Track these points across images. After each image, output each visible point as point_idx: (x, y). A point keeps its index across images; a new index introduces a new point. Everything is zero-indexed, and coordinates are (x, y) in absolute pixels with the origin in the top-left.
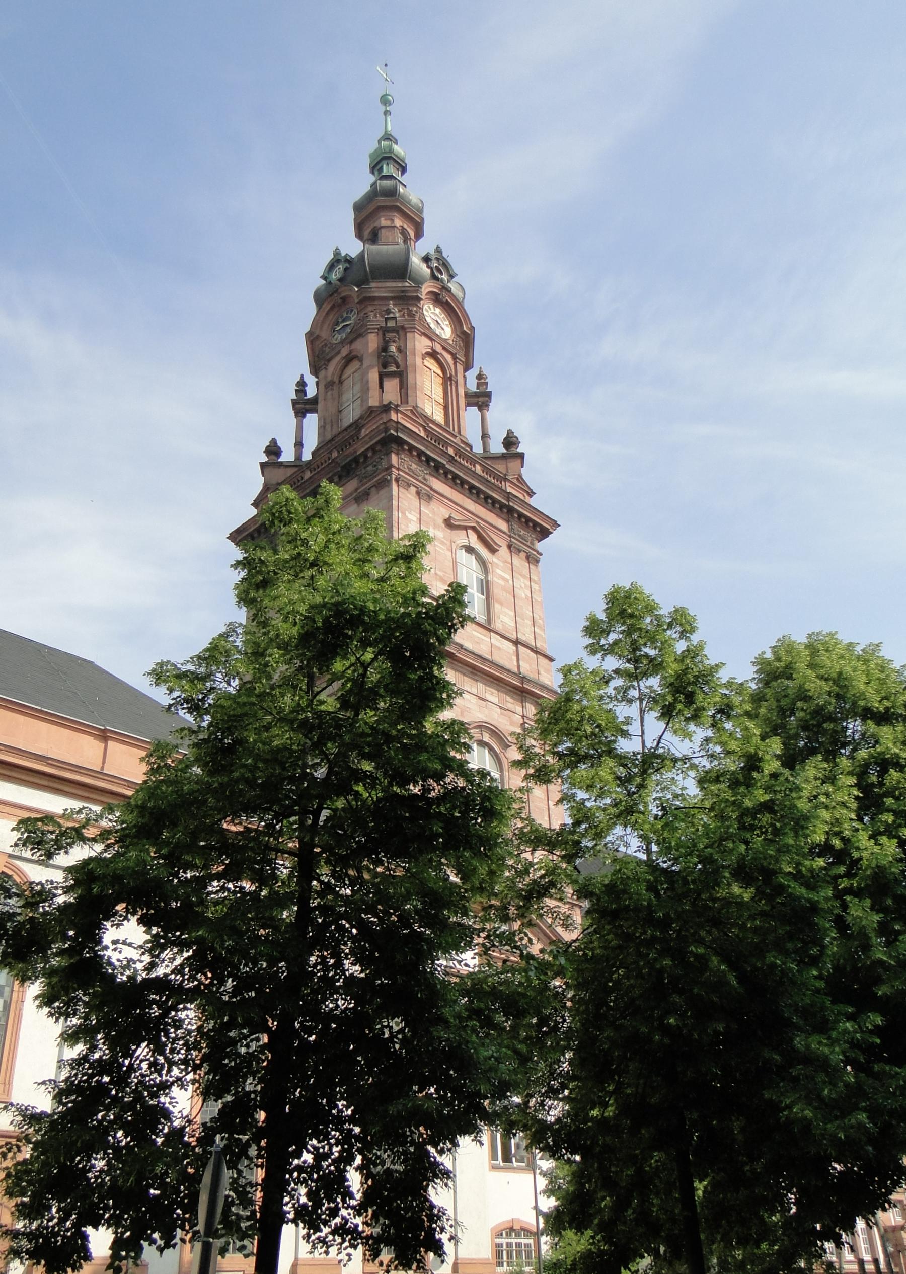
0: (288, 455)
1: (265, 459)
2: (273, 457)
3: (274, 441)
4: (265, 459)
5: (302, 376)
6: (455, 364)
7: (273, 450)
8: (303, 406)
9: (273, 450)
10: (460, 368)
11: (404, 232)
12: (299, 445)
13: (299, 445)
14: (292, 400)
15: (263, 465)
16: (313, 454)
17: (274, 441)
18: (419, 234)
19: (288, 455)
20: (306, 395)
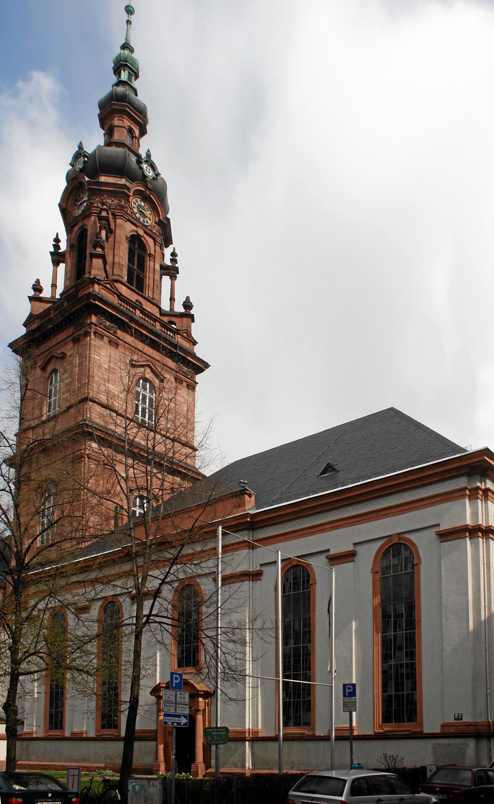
0: (46, 293)
1: (32, 293)
2: (37, 293)
3: (38, 281)
4: (32, 293)
5: (57, 234)
6: (155, 244)
7: (37, 288)
8: (57, 257)
9: (37, 288)
10: (158, 248)
11: (130, 131)
12: (54, 286)
13: (54, 286)
14: (50, 252)
15: (31, 299)
16: (61, 295)
17: (38, 281)
18: (143, 132)
19: (46, 293)
20: (60, 249)
